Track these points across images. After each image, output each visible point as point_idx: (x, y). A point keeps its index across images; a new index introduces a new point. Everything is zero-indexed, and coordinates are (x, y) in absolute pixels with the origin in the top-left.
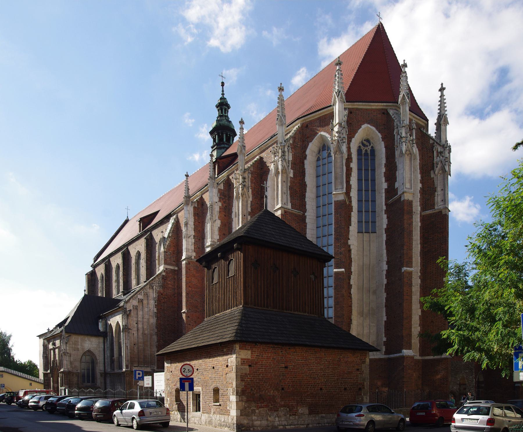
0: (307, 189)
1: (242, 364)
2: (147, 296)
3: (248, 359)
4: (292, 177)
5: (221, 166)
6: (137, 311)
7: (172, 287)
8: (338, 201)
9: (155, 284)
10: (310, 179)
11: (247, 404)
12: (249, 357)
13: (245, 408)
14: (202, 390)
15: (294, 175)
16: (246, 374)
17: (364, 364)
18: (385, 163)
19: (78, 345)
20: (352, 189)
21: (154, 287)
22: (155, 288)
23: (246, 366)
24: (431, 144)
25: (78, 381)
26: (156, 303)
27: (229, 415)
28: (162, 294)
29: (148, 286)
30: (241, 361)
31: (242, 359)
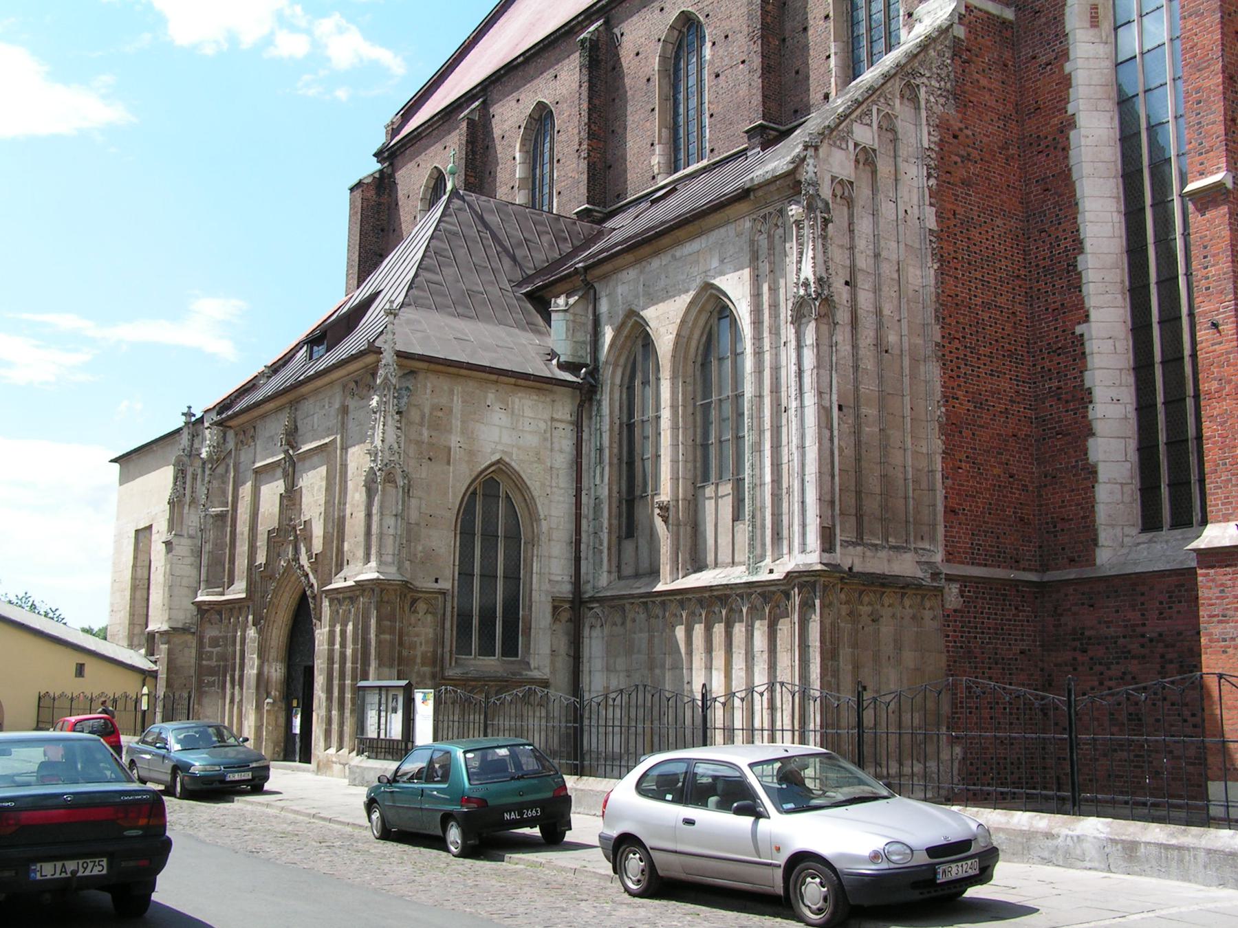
2: (890, 136)
6: (851, 216)
7: (994, 104)
19: (450, 432)
21: (923, 90)
22: (928, 101)
26: (932, 182)
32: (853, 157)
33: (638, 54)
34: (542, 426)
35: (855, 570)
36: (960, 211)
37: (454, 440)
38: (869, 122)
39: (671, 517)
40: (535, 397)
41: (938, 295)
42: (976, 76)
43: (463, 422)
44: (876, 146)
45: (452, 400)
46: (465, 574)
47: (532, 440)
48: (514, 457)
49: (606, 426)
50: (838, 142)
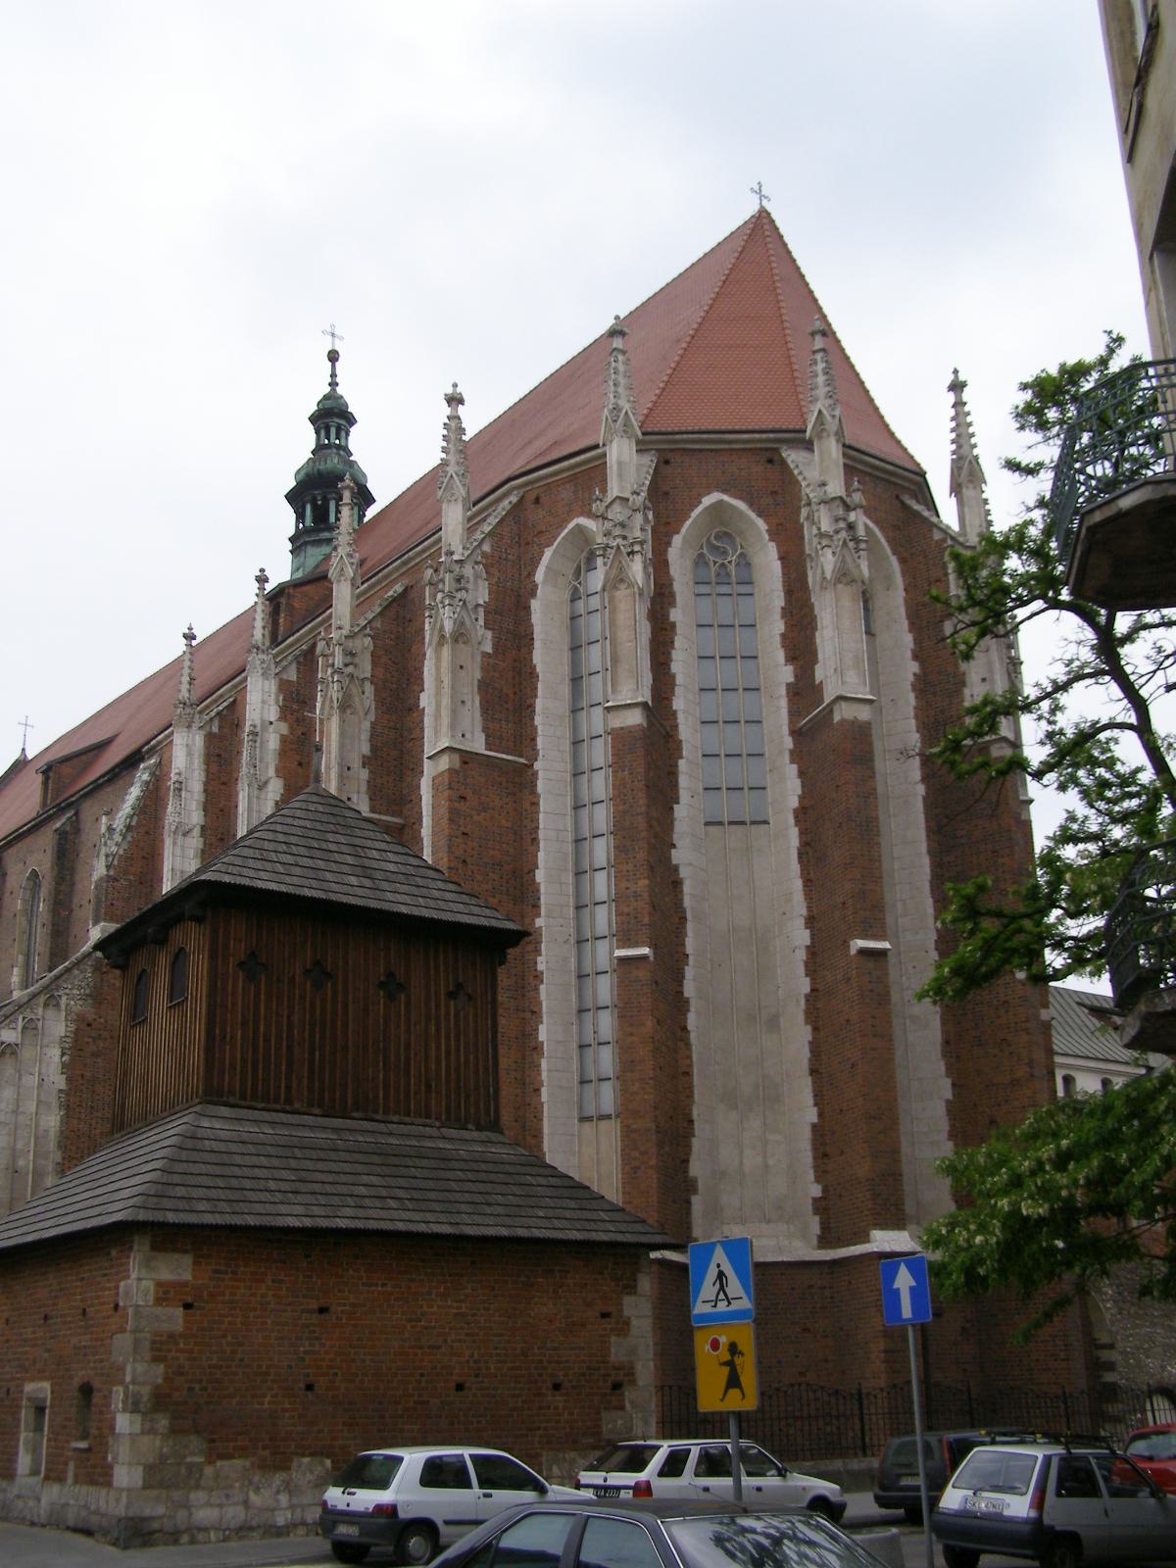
0: (540, 685)
1: (160, 1301)
2: (35, 1032)
3: (185, 1284)
4: (490, 651)
5: (296, 605)
8: (622, 728)
9: (67, 991)
10: (547, 657)
11: (171, 1443)
12: (187, 1276)
13: (163, 1458)
14: (52, 1392)
15: (496, 646)
16: (171, 1336)
17: (628, 1294)
18: (783, 604)
20: (676, 688)
21: (64, 998)
22: (67, 1005)
23: (170, 1310)
24: (937, 542)
27: (109, 1484)
28: (89, 1025)
29: (42, 999)
30: (157, 1292)
31: (159, 1284)
36: (88, 1074)
41: (61, 1132)
42: (112, 981)
44: (19, 1042)
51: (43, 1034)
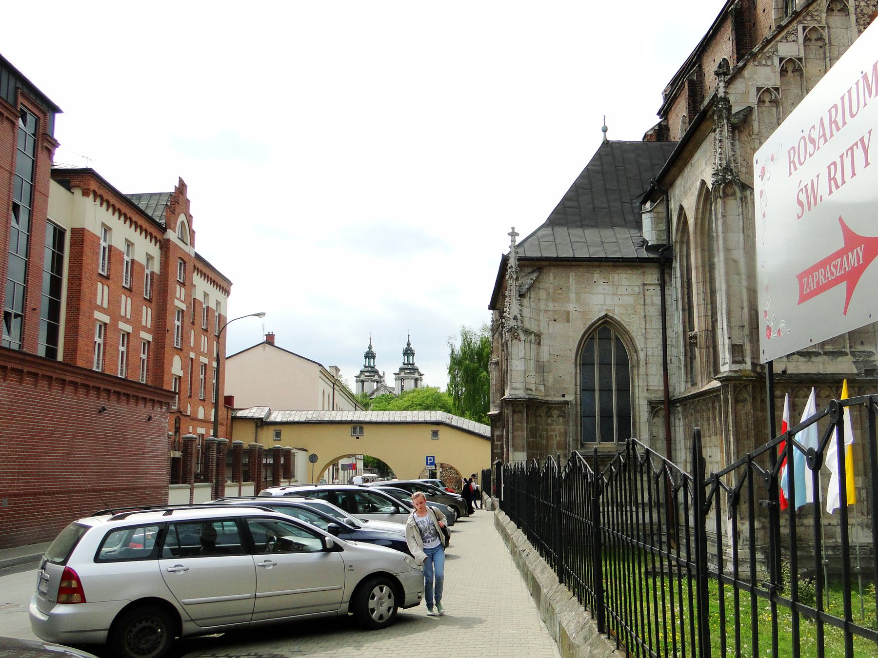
2: (820, 43)
22: (857, 7)
25: (566, 433)
32: (778, 69)
33: (764, 11)
34: (637, 289)
35: (788, 372)
37: (571, 307)
38: (795, 38)
39: (698, 342)
40: (630, 272)
43: (577, 294)
44: (802, 55)
45: (569, 282)
46: (586, 389)
47: (630, 300)
48: (616, 313)
49: (679, 285)
50: (764, 62)
51: (830, 45)
